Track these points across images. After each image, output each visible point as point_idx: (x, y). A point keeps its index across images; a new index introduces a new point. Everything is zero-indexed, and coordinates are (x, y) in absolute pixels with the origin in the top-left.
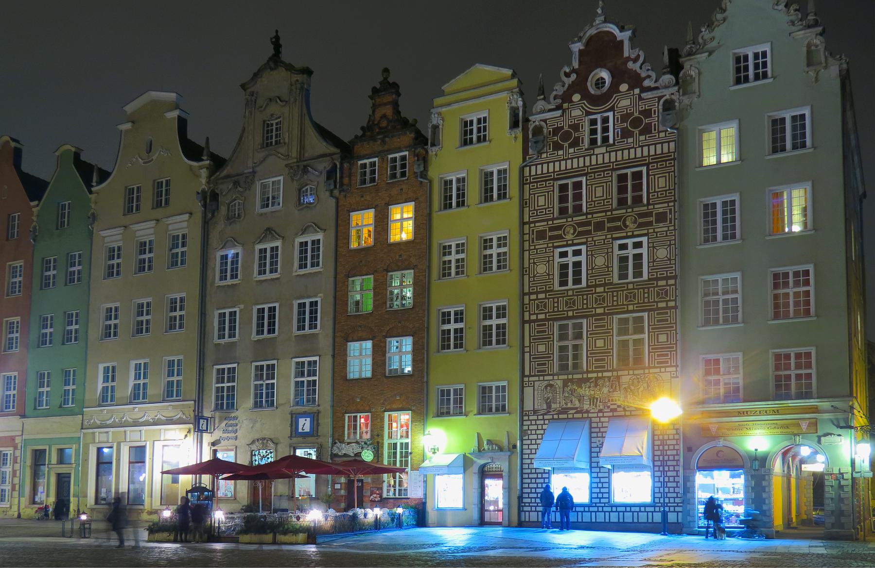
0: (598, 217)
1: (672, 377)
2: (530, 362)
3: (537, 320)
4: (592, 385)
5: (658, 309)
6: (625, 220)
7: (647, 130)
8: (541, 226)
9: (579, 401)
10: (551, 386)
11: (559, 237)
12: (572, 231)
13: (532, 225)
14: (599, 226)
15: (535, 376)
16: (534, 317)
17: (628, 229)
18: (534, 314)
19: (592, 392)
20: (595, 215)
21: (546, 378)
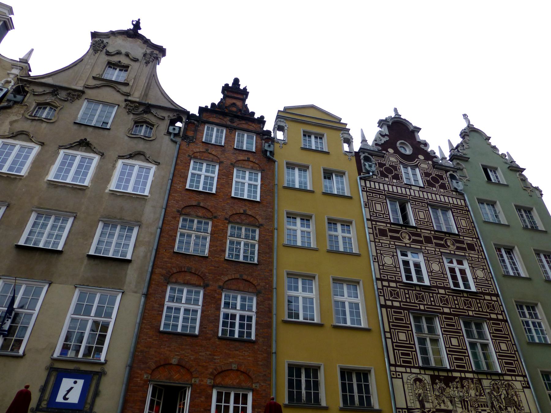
0: (426, 233)
1: (523, 387)
2: (394, 350)
3: (392, 307)
4: (459, 386)
5: (491, 319)
6: (446, 242)
7: (443, 186)
8: (382, 226)
9: (451, 402)
10: (420, 380)
11: (398, 239)
12: (408, 237)
13: (374, 223)
14: (428, 240)
15: (401, 366)
16: (389, 303)
17: (450, 249)
18: (389, 300)
19: (461, 394)
20: (422, 231)
21: (414, 370)
